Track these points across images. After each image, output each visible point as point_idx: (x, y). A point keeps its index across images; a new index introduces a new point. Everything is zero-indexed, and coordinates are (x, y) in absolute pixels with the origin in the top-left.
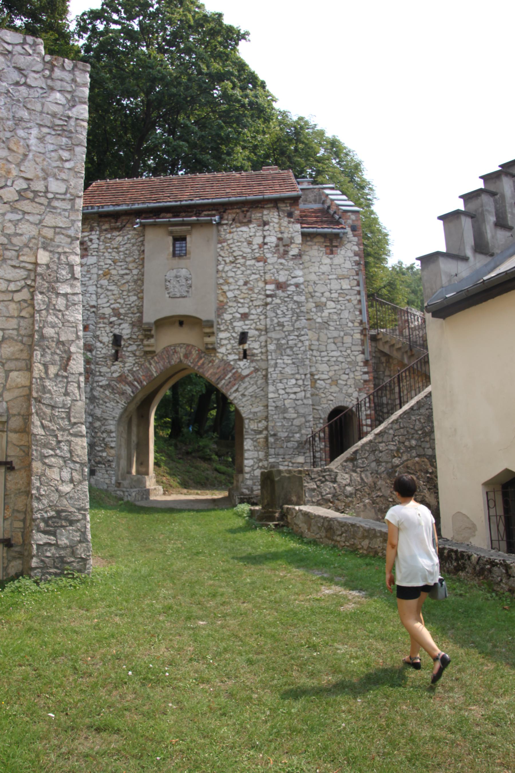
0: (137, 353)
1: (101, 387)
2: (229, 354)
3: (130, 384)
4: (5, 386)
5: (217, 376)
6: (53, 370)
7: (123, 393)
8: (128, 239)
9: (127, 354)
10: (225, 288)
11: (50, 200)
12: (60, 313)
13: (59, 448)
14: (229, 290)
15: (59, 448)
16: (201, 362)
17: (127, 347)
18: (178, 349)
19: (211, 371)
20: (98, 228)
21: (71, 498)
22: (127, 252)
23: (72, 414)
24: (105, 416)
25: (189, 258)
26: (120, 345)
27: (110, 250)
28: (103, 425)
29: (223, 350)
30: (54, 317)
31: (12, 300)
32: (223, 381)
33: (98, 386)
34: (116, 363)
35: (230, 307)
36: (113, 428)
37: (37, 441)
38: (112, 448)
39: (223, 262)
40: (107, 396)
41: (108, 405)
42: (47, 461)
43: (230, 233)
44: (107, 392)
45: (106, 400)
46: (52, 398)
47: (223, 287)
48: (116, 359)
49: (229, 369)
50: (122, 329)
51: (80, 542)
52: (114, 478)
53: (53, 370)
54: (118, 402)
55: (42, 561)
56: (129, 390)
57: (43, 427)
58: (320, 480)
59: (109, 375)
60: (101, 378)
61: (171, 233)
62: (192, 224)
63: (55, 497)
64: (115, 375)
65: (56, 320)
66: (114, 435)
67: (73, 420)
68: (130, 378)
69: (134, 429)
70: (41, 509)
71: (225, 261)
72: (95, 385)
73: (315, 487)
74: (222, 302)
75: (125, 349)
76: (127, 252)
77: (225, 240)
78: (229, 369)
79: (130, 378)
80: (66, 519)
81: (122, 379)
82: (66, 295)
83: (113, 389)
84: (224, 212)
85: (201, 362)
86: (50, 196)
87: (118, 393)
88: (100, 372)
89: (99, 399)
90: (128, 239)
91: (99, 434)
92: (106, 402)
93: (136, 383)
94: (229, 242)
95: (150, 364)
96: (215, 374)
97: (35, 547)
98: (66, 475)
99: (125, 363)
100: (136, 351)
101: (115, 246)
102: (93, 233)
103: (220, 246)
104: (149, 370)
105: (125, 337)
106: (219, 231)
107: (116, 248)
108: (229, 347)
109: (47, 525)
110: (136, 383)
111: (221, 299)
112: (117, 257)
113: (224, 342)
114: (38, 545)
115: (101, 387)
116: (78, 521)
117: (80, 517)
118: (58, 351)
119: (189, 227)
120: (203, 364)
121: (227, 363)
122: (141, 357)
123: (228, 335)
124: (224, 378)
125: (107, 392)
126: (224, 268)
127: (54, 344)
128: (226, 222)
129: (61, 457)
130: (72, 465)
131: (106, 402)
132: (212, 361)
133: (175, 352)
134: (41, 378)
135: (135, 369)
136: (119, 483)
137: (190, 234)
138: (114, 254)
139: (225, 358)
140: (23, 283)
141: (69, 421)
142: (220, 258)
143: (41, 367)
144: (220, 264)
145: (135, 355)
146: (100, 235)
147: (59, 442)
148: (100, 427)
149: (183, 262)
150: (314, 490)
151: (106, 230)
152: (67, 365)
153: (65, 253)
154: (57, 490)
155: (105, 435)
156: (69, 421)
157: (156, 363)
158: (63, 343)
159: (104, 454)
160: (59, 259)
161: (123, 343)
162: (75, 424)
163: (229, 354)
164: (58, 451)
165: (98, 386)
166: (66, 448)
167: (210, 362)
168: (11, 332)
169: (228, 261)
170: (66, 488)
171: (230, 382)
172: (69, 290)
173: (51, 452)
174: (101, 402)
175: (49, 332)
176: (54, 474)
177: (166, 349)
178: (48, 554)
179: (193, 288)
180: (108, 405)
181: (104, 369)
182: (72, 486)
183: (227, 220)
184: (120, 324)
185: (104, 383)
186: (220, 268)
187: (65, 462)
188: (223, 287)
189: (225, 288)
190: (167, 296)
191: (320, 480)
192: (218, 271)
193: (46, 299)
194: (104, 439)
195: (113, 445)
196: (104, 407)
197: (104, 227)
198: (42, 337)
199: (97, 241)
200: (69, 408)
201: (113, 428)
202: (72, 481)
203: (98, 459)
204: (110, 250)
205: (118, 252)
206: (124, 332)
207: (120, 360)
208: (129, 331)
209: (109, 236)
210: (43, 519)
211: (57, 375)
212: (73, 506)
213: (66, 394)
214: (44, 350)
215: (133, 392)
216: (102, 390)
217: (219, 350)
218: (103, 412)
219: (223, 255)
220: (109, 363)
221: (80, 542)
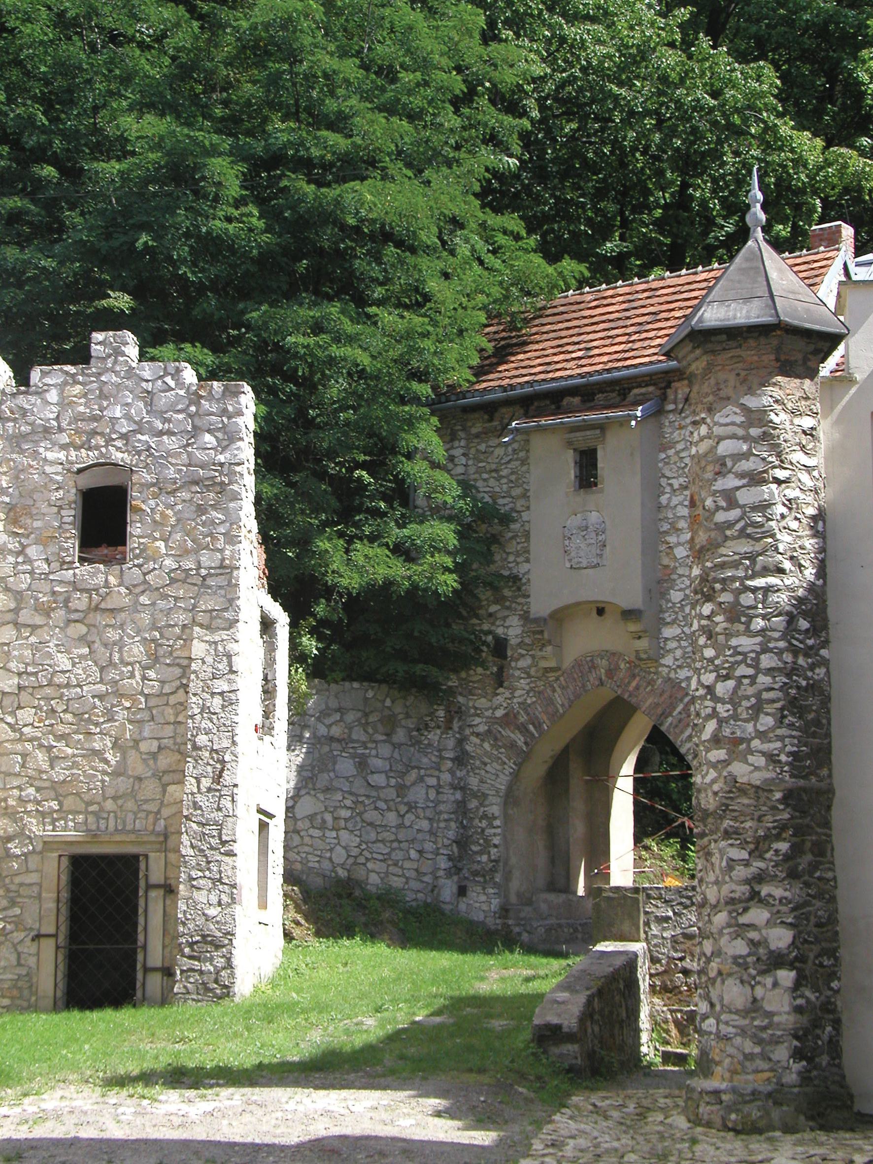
0: (533, 671)
1: (477, 735)
2: (679, 667)
3: (523, 729)
4: (162, 802)
5: (659, 711)
6: (206, 783)
7: (513, 745)
8: (514, 450)
9: (517, 673)
10: (672, 539)
11: (204, 578)
12: (214, 717)
13: (209, 869)
14: (679, 544)
15: (209, 869)
16: (634, 684)
17: (517, 660)
18: (598, 661)
19: (650, 701)
20: (462, 434)
21: (217, 922)
22: (513, 477)
23: (224, 831)
24: (485, 788)
25: (602, 491)
26: (505, 657)
27: (485, 476)
28: (482, 805)
29: (668, 660)
30: (208, 722)
31: (167, 704)
32: (670, 719)
33: (473, 733)
34: (501, 690)
35: (681, 576)
36: (495, 810)
37: (186, 862)
38: (495, 846)
39: (668, 489)
40: (486, 752)
41: (488, 768)
42: (195, 883)
43: (681, 428)
44: (486, 745)
45: (486, 760)
46: (203, 815)
47: (668, 539)
48: (501, 685)
49: (679, 696)
50: (507, 627)
51: (224, 968)
52: (495, 902)
53: (206, 783)
54: (505, 763)
55: (185, 987)
56: (520, 740)
57: (192, 846)
58: (681, 904)
59: (488, 713)
60: (477, 720)
61: (570, 443)
62: (602, 427)
63: (200, 921)
64: (499, 713)
65: (210, 725)
66: (497, 823)
67: (224, 838)
68: (523, 718)
69: (578, 805)
70: (186, 932)
71: (671, 485)
72: (467, 731)
73: (671, 914)
74: (667, 567)
75: (513, 664)
76: (513, 477)
77: (672, 445)
78: (679, 696)
79: (523, 718)
80: (211, 943)
81: (509, 719)
82: (222, 694)
83: (496, 739)
84: (668, 386)
85: (634, 684)
86: (203, 572)
87: (505, 746)
88: (476, 709)
89: (473, 757)
90: (514, 450)
91: (476, 822)
92: (485, 764)
93: (531, 727)
94: (680, 446)
95: (554, 691)
96: (657, 705)
97: (178, 972)
98: (214, 899)
99: (513, 690)
100: (529, 667)
101: (494, 466)
102: (456, 443)
103: (663, 456)
104: (551, 702)
105: (513, 642)
106: (661, 426)
107: (496, 471)
108: (679, 653)
109: (193, 950)
110: (531, 727)
111: (666, 561)
112: (497, 489)
113: (672, 645)
114: (182, 971)
115: (477, 735)
116: (224, 946)
117: (226, 942)
118: (211, 762)
119: (598, 431)
120: (637, 688)
121: (675, 685)
122: (539, 678)
123: (679, 631)
124: (670, 714)
125: (486, 745)
126: (670, 499)
127: (207, 754)
128: (671, 407)
129: (209, 878)
130: (221, 887)
131: (485, 764)
132: (651, 683)
133: (593, 667)
134: (192, 794)
135: (529, 701)
136: (507, 911)
137: (603, 442)
138: (492, 482)
139: (672, 675)
140: (178, 683)
141: (220, 839)
142: (663, 482)
143: (193, 781)
144: (664, 493)
145: (529, 676)
146: (467, 447)
147: (209, 862)
148: (477, 808)
149: (592, 498)
150: (667, 919)
151: (477, 436)
152: (220, 776)
153: (222, 641)
154: (204, 914)
155: (484, 823)
156: (220, 839)
157: (563, 688)
158: (216, 751)
159: (484, 858)
160: (216, 650)
161: (509, 653)
162: (227, 842)
163: (679, 667)
164: (207, 873)
165: (473, 733)
166: (215, 869)
167: (649, 683)
168: (166, 741)
169: (676, 486)
170: (212, 912)
171: (680, 721)
172: (226, 688)
173: (200, 874)
174: (478, 763)
175: (202, 740)
176: (201, 897)
177: (578, 664)
178: (192, 980)
179: (608, 548)
180: (488, 768)
181: (482, 703)
182: (219, 909)
183: (675, 402)
184: (505, 618)
185: (482, 729)
186: (664, 499)
187: (214, 883)
188: (668, 539)
189: (672, 539)
190: (568, 565)
191: (681, 904)
192: (660, 507)
193: (201, 702)
194: (483, 830)
195: (496, 841)
196: (483, 772)
197: (474, 431)
198: (196, 748)
199: (463, 460)
200: (221, 825)
201: (495, 810)
202: (220, 904)
203: (476, 867)
204: (485, 476)
205: (498, 479)
206: (512, 632)
207: (506, 684)
208: (518, 631)
209: (483, 447)
210: (191, 945)
211: (209, 790)
212: (220, 930)
213: (219, 809)
214: (196, 761)
215: (526, 743)
216: (477, 741)
217: (663, 661)
218: (482, 781)
219: (668, 474)
220: (489, 690)
221: (224, 968)
